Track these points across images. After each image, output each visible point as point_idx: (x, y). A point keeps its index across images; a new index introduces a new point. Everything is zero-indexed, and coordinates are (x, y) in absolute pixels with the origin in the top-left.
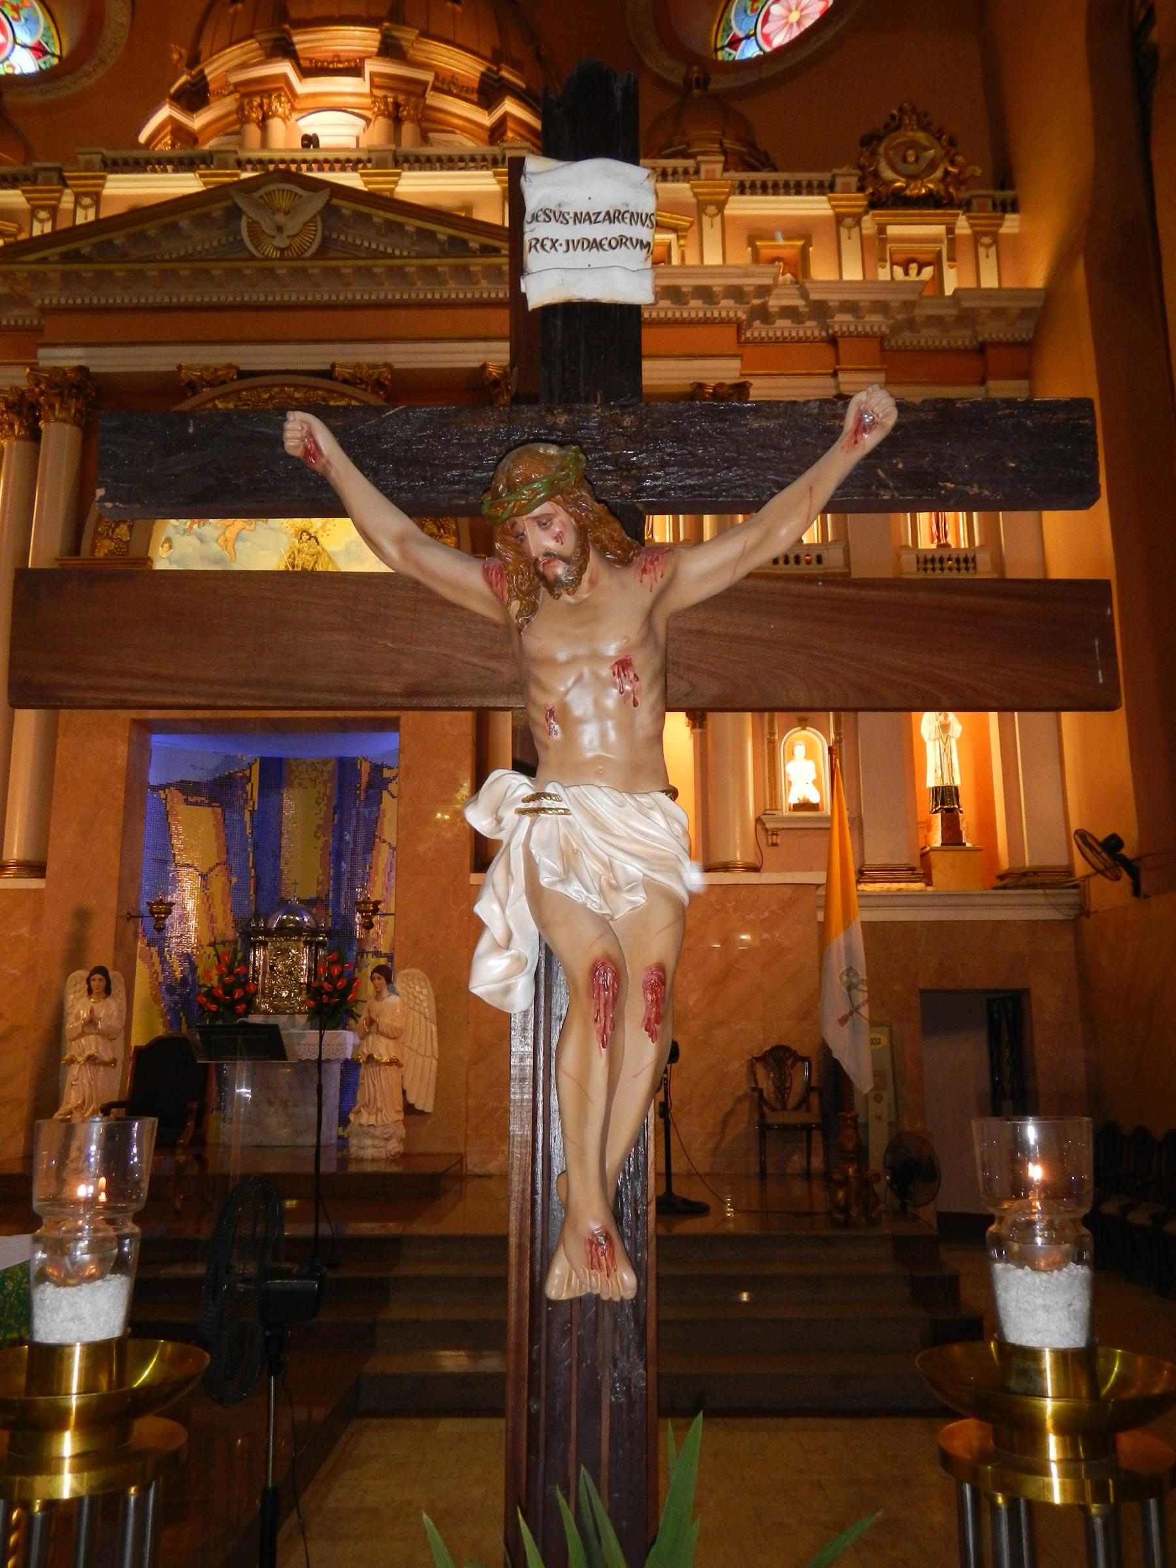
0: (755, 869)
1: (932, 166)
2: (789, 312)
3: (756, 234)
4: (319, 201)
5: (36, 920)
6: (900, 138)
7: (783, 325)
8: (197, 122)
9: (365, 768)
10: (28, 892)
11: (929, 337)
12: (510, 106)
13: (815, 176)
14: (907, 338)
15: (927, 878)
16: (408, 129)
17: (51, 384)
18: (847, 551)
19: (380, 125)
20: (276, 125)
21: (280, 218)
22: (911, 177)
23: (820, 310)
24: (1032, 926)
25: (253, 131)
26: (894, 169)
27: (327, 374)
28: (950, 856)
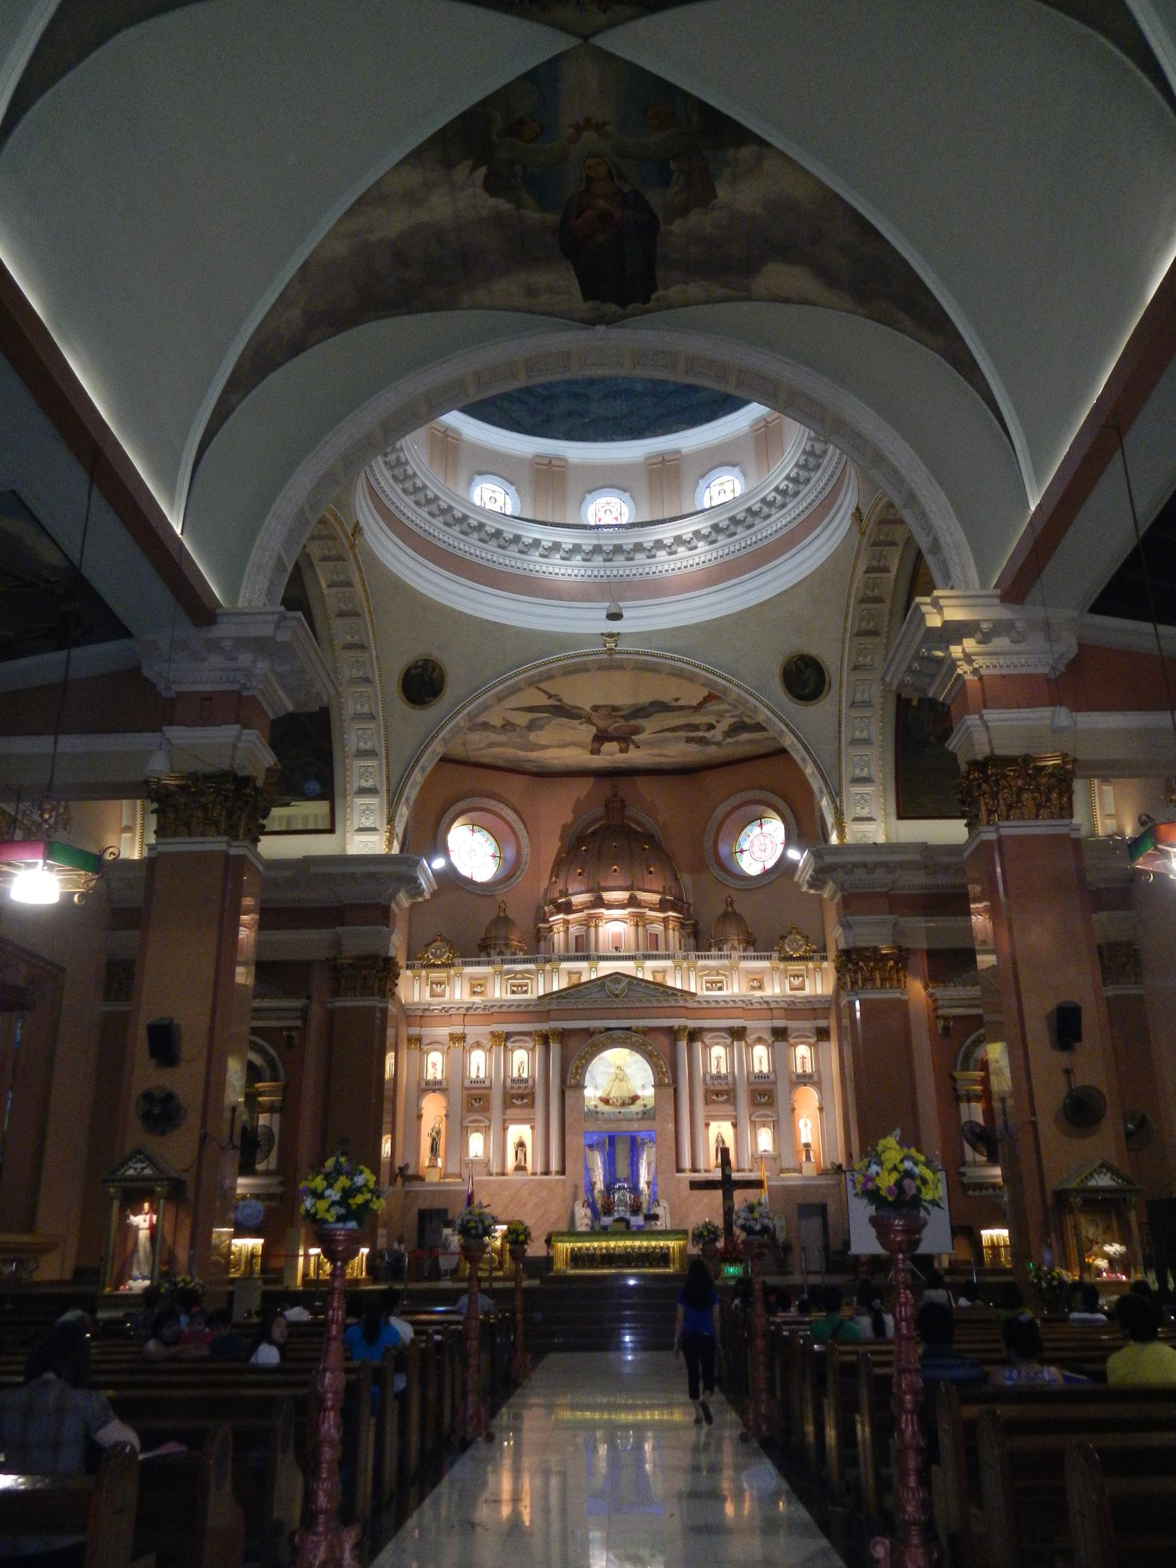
0: (751, 1171)
1: (801, 946)
2: (759, 1003)
3: (748, 972)
4: (626, 981)
5: (564, 1187)
6: (792, 937)
7: (756, 1006)
8: (571, 917)
9: (639, 1140)
10: (559, 1180)
11: (799, 1006)
12: (671, 913)
13: (765, 954)
14: (793, 1007)
15: (800, 1172)
16: (640, 929)
17: (555, 1033)
18: (776, 1075)
19: (633, 928)
20: (600, 929)
21: (617, 986)
22: (795, 950)
23: (767, 1002)
24: (828, 1187)
25: (593, 930)
26: (789, 945)
27: (629, 1029)
28: (809, 1164)
